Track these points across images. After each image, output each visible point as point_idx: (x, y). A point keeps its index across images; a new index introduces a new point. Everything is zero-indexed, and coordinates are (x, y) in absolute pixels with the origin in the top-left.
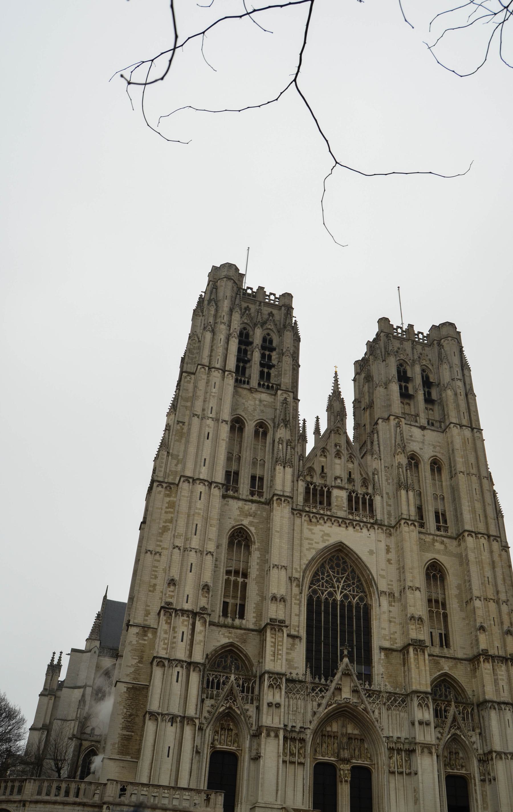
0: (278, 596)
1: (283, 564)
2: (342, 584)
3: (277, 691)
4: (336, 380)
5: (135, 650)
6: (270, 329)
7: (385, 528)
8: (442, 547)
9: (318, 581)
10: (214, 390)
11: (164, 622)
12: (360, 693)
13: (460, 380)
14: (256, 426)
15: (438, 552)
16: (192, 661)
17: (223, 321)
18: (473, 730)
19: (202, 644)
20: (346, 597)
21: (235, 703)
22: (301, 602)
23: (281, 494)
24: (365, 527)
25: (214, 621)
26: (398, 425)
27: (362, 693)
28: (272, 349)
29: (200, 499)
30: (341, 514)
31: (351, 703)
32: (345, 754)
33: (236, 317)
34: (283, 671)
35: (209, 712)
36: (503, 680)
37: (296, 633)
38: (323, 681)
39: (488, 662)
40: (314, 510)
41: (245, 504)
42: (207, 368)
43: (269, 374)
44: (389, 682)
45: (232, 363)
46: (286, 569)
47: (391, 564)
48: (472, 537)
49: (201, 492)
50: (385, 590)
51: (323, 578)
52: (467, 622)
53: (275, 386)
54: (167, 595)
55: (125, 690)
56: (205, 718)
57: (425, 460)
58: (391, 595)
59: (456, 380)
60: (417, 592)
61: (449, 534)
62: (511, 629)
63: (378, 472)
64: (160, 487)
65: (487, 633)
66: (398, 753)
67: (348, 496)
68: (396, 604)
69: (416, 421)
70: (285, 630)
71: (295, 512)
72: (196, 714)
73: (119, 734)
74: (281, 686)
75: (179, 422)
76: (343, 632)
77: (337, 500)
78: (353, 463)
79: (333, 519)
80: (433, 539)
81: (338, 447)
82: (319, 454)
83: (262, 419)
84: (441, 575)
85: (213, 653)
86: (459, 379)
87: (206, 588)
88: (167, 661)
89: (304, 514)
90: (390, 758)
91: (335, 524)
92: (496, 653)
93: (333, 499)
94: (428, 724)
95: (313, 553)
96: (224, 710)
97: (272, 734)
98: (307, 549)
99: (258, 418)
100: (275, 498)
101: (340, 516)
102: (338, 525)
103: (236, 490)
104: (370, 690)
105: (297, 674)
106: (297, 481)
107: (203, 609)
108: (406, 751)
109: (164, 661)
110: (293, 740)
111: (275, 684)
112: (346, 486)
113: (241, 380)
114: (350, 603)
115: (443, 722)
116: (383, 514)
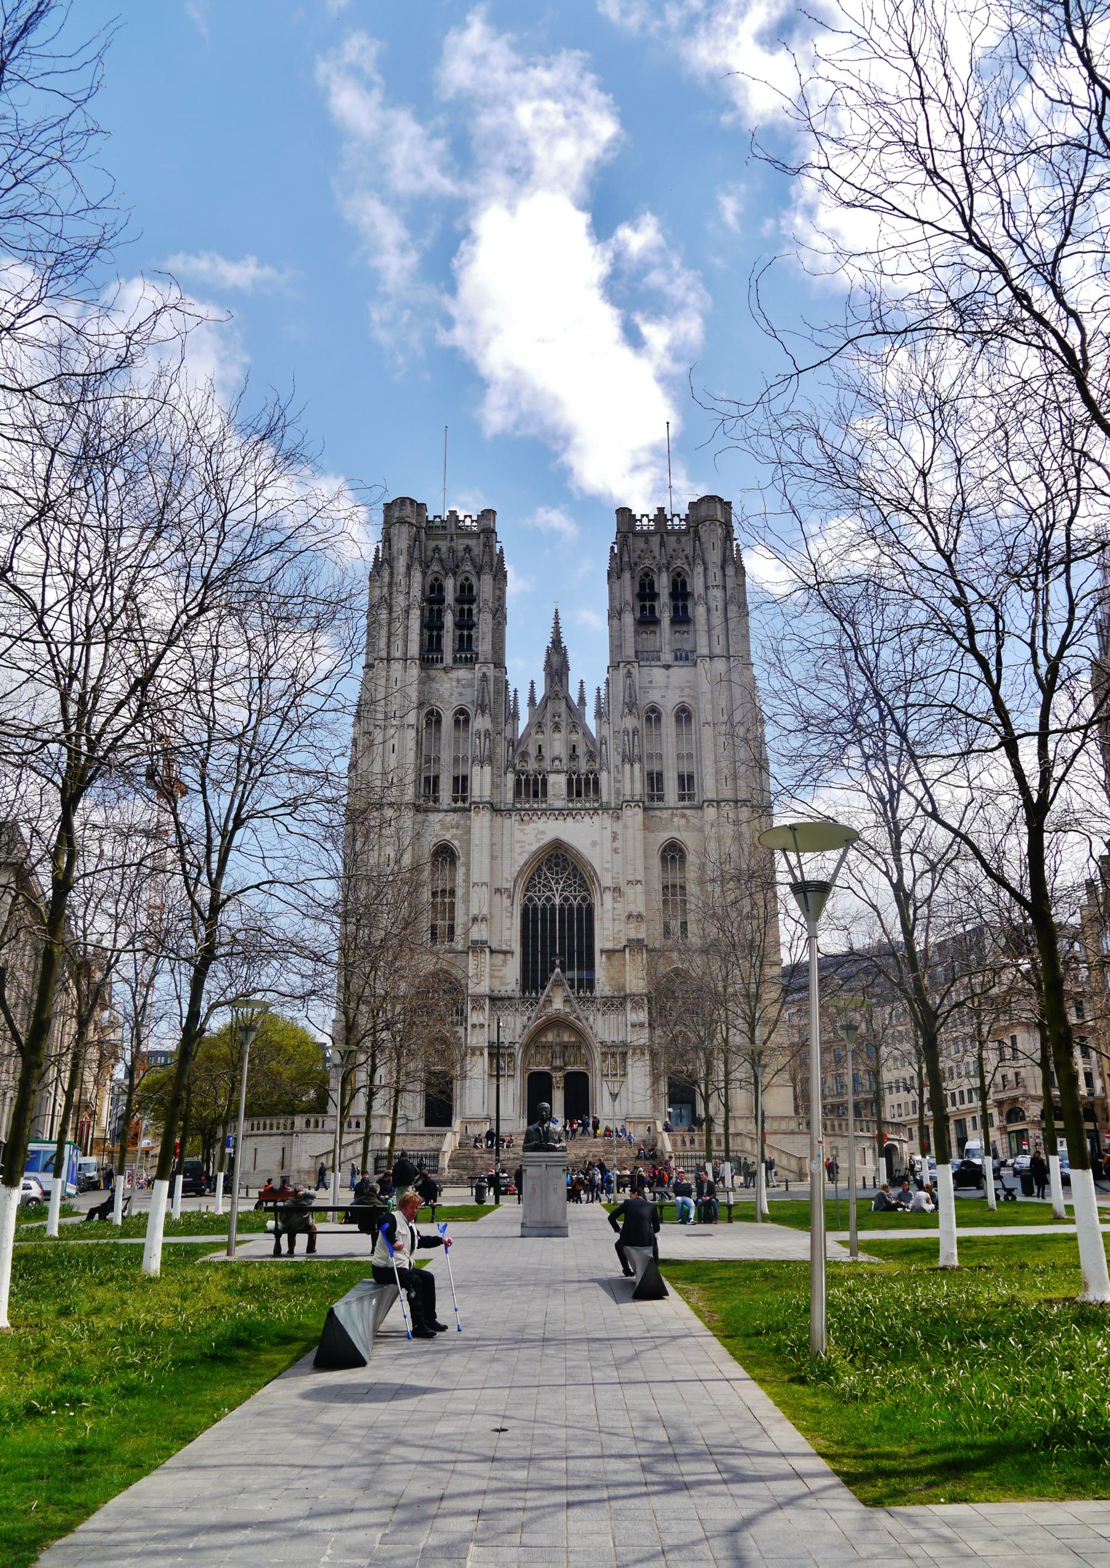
4: (557, 623)
8: (683, 821)
20: (566, 899)
26: (629, 674)
28: (472, 601)
30: (559, 804)
32: (558, 1063)
33: (417, 576)
34: (487, 992)
43: (470, 636)
58: (617, 890)
69: (659, 659)
76: (562, 938)
82: (533, 732)
93: (550, 788)
95: (526, 856)
103: (436, 800)
116: (610, 794)
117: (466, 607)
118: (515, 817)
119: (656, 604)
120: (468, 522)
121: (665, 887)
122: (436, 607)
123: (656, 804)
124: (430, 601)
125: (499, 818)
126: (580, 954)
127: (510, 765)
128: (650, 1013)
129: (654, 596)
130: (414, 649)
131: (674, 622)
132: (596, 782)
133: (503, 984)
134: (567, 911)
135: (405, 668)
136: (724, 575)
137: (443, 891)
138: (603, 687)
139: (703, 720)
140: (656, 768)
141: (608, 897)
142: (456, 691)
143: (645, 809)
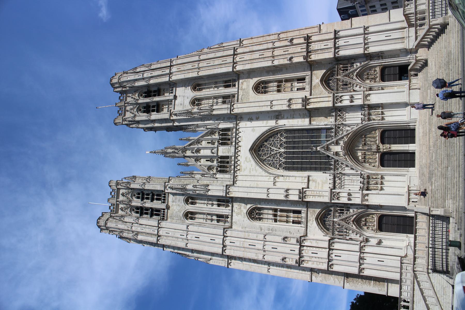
0: (285, 194)
1: (266, 192)
2: (274, 148)
3: (341, 195)
5: (325, 278)
6: (131, 195)
8: (245, 83)
11: (307, 264)
12: (338, 139)
13: (143, 74)
14: (188, 204)
15: (248, 86)
16: (328, 248)
17: (130, 228)
18: (353, 63)
19: (318, 241)
20: (281, 145)
21: (350, 218)
23: (225, 192)
24: (239, 134)
25: (304, 230)
29: (234, 243)
30: (233, 149)
31: (344, 145)
32: (374, 147)
35: (356, 235)
36: (320, 46)
37: (306, 179)
39: (311, 55)
40: (233, 167)
41: (234, 211)
42: (159, 238)
45: (153, 222)
46: (269, 189)
47: (259, 117)
48: (236, 66)
49: (230, 242)
51: (272, 161)
52: (288, 67)
53: (163, 193)
54: (292, 263)
55: (348, 284)
56: (360, 237)
59: (143, 77)
61: (237, 78)
62: (289, 40)
63: (205, 126)
64: (231, 264)
65: (293, 56)
66: (371, 115)
67: (221, 145)
68: (282, 114)
69: (171, 101)
70: (305, 190)
71: (235, 180)
72: (358, 245)
73: (373, 287)
74: (337, 192)
78: (202, 141)
79: (237, 155)
81: (194, 151)
83: (184, 200)
84: (263, 84)
85: (322, 231)
86: (143, 75)
87: (285, 238)
88: (330, 263)
89: (235, 174)
90: (374, 120)
91: (239, 154)
92: (305, 50)
93: (224, 155)
94: (352, 97)
95: (258, 168)
96: (355, 225)
98: (256, 172)
99: (183, 203)
100: (228, 196)
101: (234, 150)
102: (239, 152)
104: (335, 133)
105: (330, 180)
106: (217, 178)
107: (297, 241)
108: (369, 110)
109: (329, 265)
111: (337, 196)
115: (350, 83)
118: (238, 173)
119: (152, 105)
120: (113, 194)
124: (141, 214)
126: (312, 137)
131: (159, 95)
140: (220, 100)
142: (178, 203)
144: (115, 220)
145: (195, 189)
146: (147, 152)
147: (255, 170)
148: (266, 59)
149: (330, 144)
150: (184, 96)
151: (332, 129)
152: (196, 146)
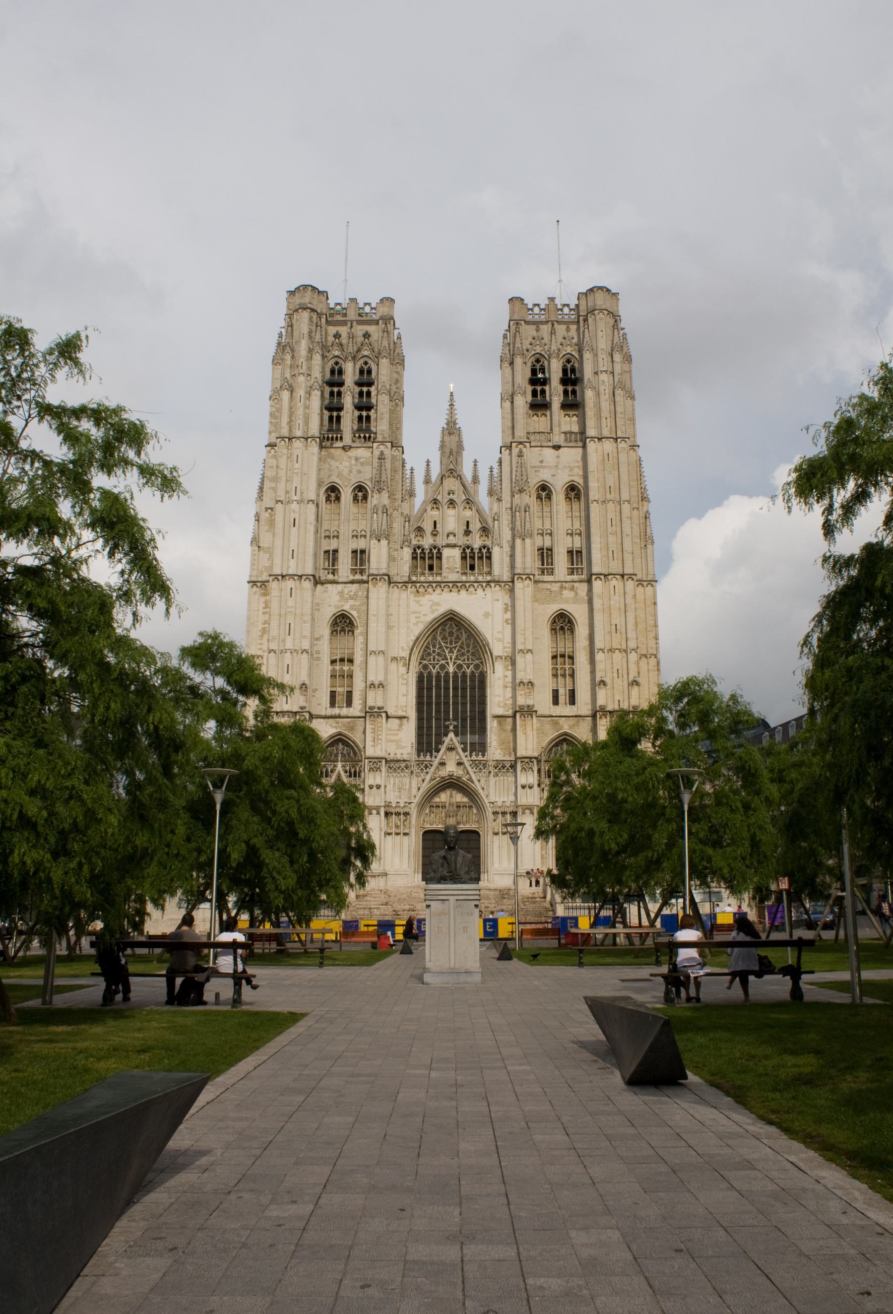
0: (376, 683)
1: (380, 649)
6: (366, 356)
7: (503, 584)
9: (429, 654)
10: (297, 466)
13: (606, 372)
15: (567, 601)
17: (301, 371)
20: (460, 667)
22: (407, 680)
23: (375, 572)
26: (520, 455)
27: (467, 764)
28: (370, 384)
30: (453, 577)
37: (403, 714)
38: (428, 758)
40: (422, 579)
42: (287, 440)
43: (368, 418)
44: (501, 749)
48: (601, 579)
50: (501, 654)
51: (434, 651)
57: (559, 489)
60: (529, 654)
62: (637, 679)
71: (400, 585)
75: (267, 509)
76: (455, 704)
77: (448, 561)
79: (443, 585)
80: (561, 587)
82: (429, 508)
91: (446, 589)
92: (617, 708)
97: (374, 812)
107: (301, 708)
110: (398, 814)
112: (459, 544)
113: (332, 438)
114: (464, 674)
117: (365, 389)
118: (411, 589)
119: (547, 388)
120: (367, 309)
121: (554, 657)
122: (336, 389)
123: (546, 578)
125: (397, 590)
126: (473, 719)
127: (406, 541)
128: (540, 776)
129: (545, 382)
130: (314, 428)
131: (565, 406)
132: (489, 558)
133: (399, 747)
134: (460, 678)
135: (306, 446)
136: (613, 362)
137: (342, 660)
138: (496, 466)
139: (591, 498)
140: (548, 544)
141: (499, 667)
143: (535, 582)
144: (314, 328)
145: (380, 512)
146: (452, 385)
147: (418, 622)
148: (608, 637)
149: (458, 753)
150: (557, 466)
151: (483, 755)
152: (464, 498)
